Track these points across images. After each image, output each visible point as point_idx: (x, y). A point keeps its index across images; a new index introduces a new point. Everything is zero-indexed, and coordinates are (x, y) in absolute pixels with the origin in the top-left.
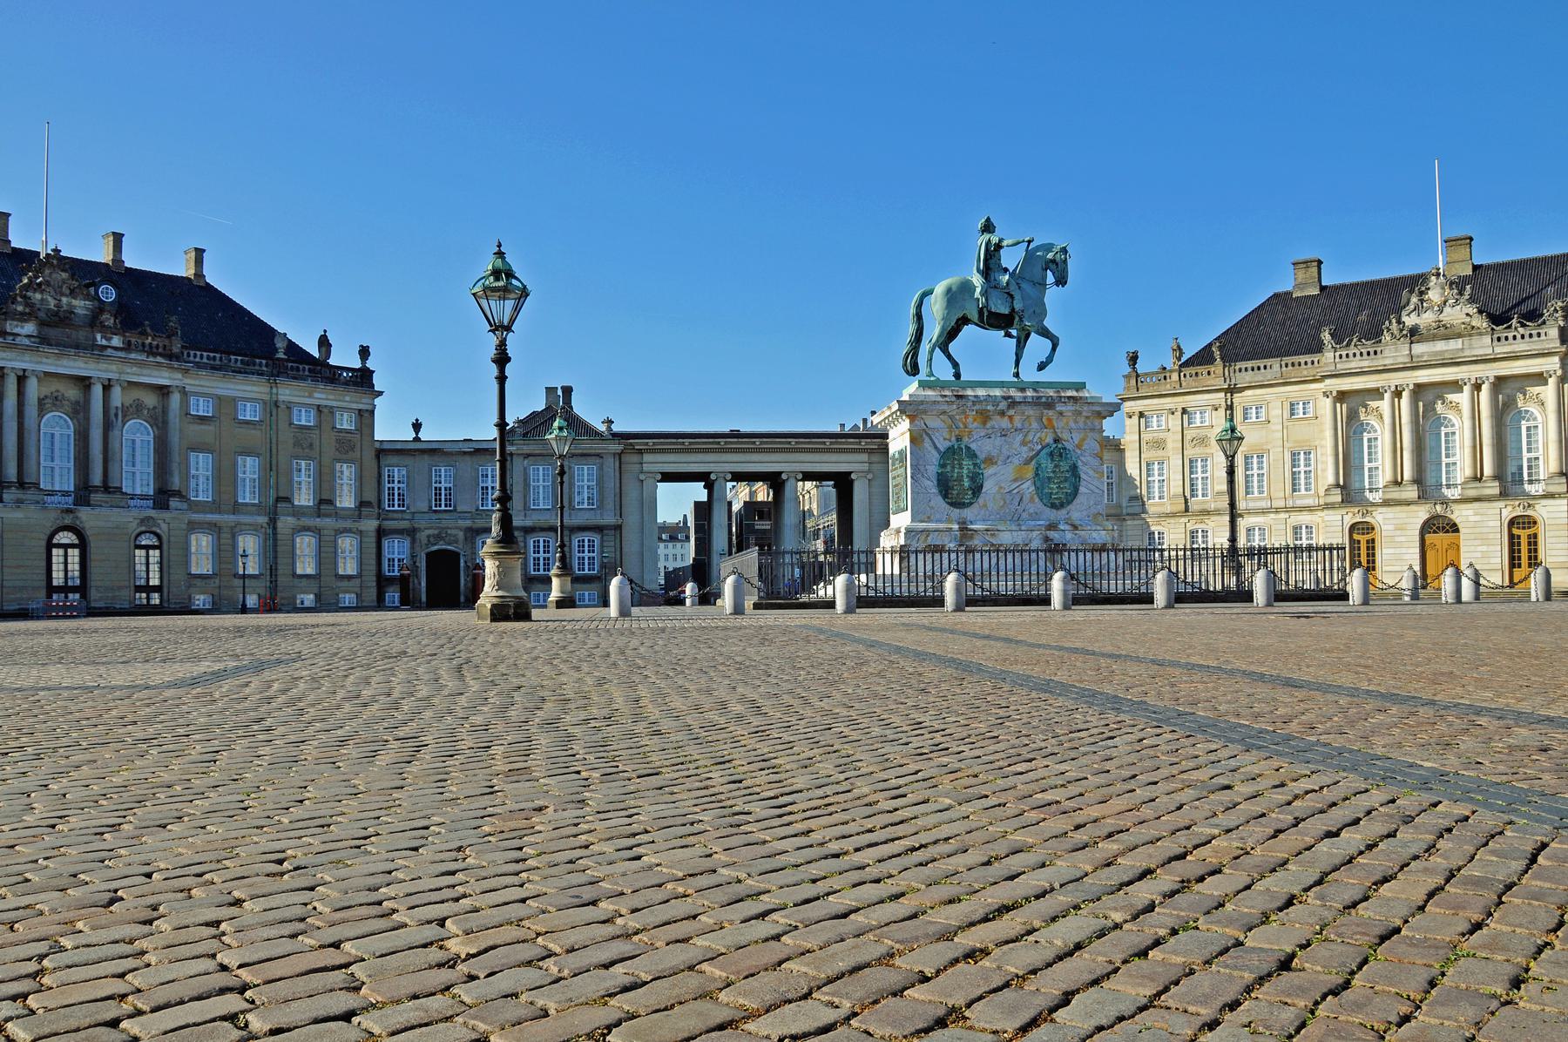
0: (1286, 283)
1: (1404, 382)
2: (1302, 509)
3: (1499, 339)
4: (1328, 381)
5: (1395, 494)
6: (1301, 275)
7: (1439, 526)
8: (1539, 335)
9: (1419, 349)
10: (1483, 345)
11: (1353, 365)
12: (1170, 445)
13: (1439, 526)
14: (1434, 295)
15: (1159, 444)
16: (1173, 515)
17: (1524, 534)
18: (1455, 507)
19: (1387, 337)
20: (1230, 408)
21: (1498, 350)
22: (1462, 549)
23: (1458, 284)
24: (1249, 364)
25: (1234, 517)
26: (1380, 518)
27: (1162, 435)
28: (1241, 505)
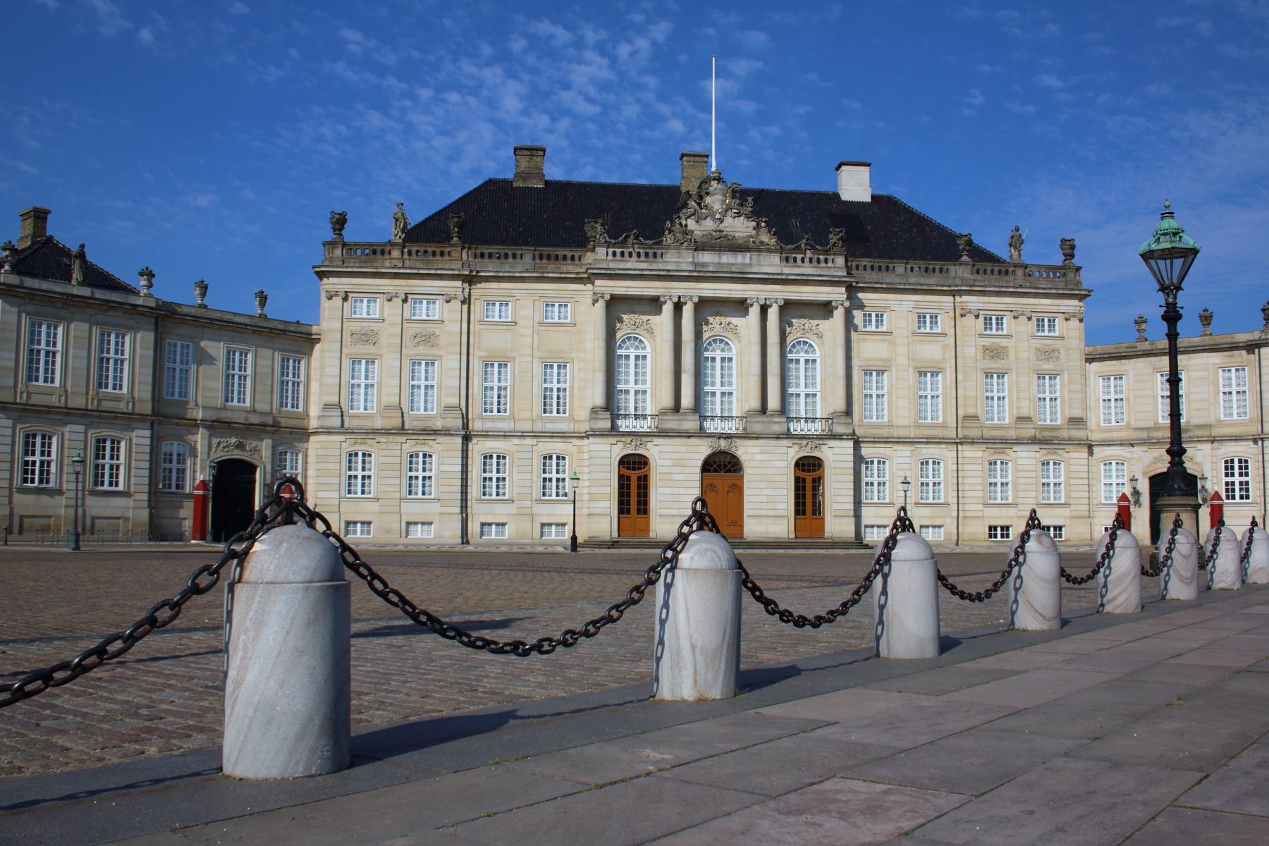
0: (502, 166)
1: (690, 293)
2: (553, 435)
3: (787, 260)
4: (598, 282)
5: (672, 423)
6: (524, 162)
7: (722, 467)
8: (826, 261)
9: (707, 257)
10: (771, 264)
11: (629, 265)
12: (384, 340)
13: (722, 467)
14: (715, 201)
15: (368, 338)
16: (387, 432)
17: (809, 477)
18: (739, 442)
19: (668, 239)
20: (467, 301)
21: (787, 270)
22: (746, 491)
23: (740, 195)
24: (494, 249)
25: (467, 438)
26: (657, 452)
27: (374, 326)
28: (476, 425)
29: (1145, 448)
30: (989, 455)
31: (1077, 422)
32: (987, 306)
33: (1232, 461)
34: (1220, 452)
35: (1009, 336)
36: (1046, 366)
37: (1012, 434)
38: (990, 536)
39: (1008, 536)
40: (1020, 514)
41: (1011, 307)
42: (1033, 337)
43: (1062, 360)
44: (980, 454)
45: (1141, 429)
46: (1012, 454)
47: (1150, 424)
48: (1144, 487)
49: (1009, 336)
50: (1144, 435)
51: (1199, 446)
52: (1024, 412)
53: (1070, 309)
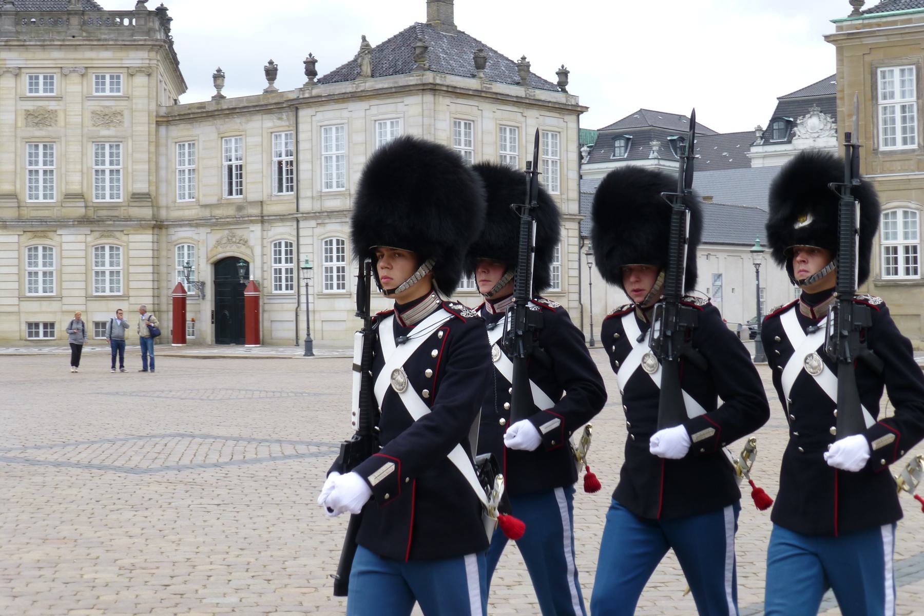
29: (209, 230)
30: (27, 240)
31: (138, 198)
32: (31, 63)
34: (270, 233)
35: (58, 98)
36: (104, 132)
37: (55, 213)
38: (30, 334)
39: (52, 334)
40: (65, 308)
41: (60, 63)
42: (90, 98)
43: (127, 123)
44: (15, 239)
45: (205, 206)
46: (57, 238)
47: (213, 200)
48: (206, 274)
49: (58, 98)
50: (206, 213)
52: (75, 188)
53: (136, 63)
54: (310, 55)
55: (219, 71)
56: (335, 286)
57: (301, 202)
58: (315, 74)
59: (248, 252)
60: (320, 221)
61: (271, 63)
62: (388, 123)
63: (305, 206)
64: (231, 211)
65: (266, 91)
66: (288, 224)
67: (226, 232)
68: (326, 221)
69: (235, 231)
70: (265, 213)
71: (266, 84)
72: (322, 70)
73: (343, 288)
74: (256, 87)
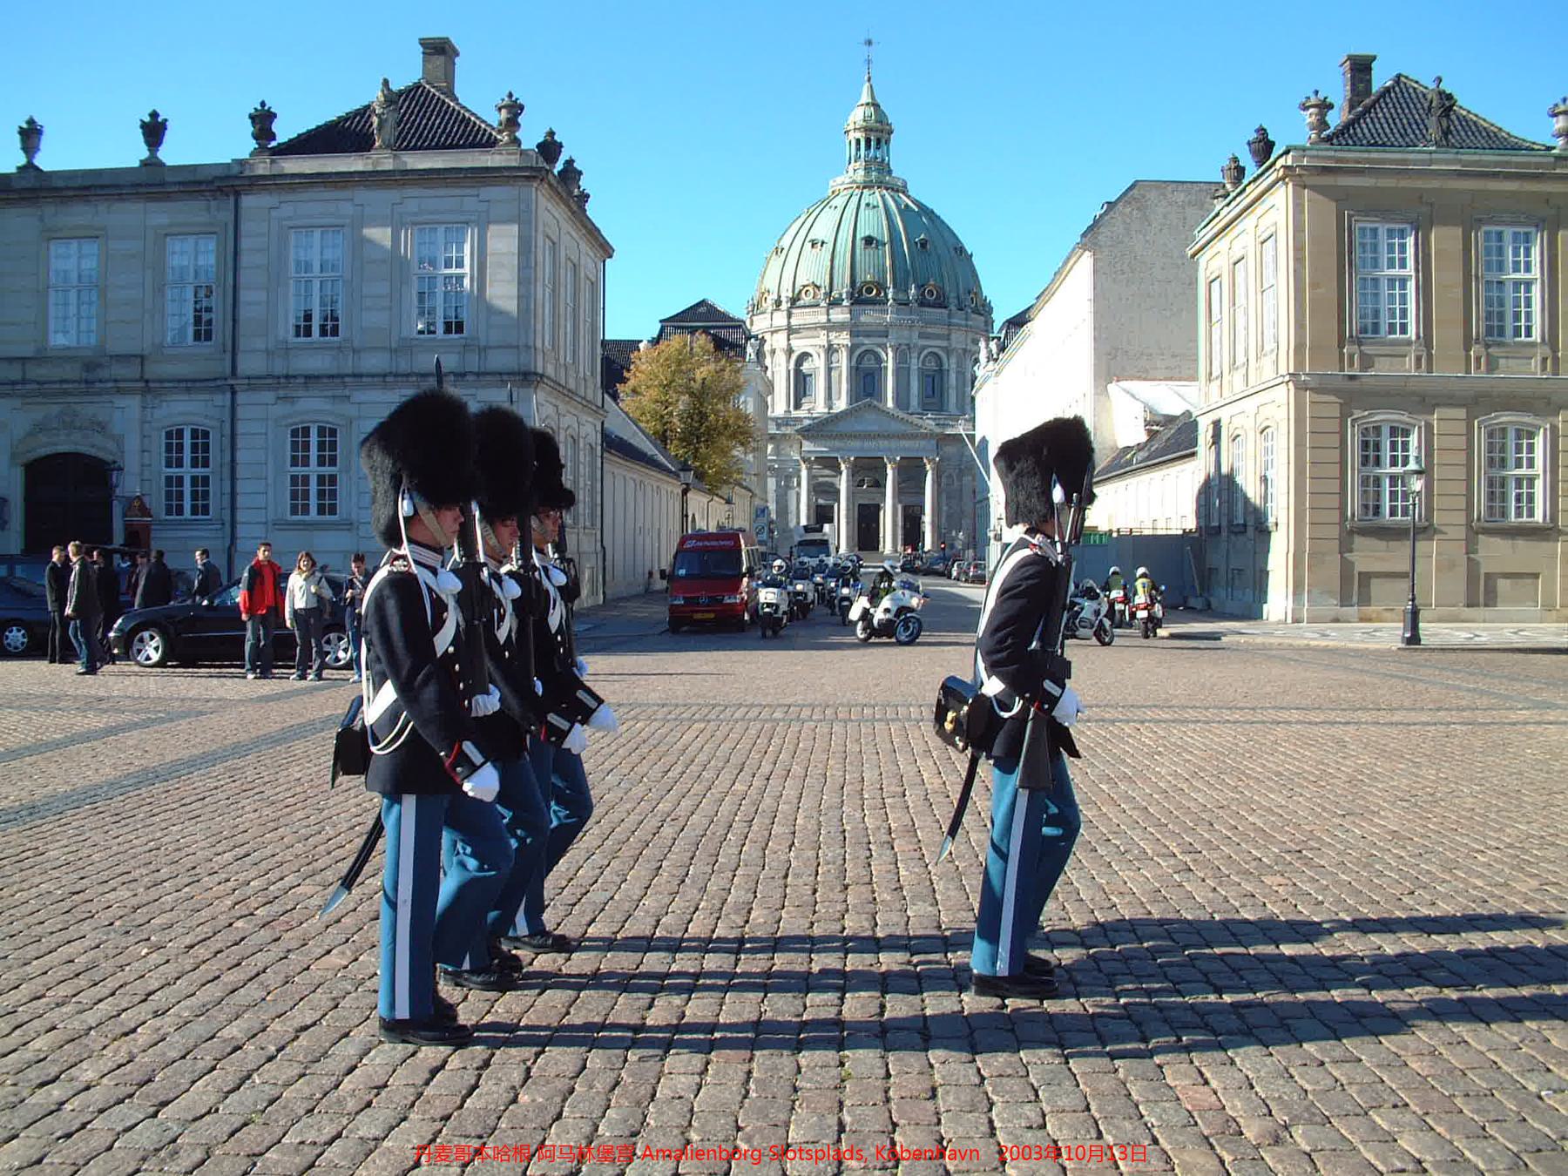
29: (17, 403)
33: (180, 433)
34: (158, 413)
47: (28, 351)
51: (120, 401)
54: (263, 104)
55: (31, 122)
56: (313, 509)
57: (240, 358)
58: (273, 137)
59: (111, 445)
60: (281, 393)
61: (154, 115)
62: (441, 229)
63: (250, 364)
64: (71, 371)
65: (144, 163)
66: (202, 397)
67: (55, 409)
68: (300, 393)
69: (78, 408)
70: (490, 352)
71: (143, 152)
72: (284, 131)
73: (333, 510)
74: (129, 153)
